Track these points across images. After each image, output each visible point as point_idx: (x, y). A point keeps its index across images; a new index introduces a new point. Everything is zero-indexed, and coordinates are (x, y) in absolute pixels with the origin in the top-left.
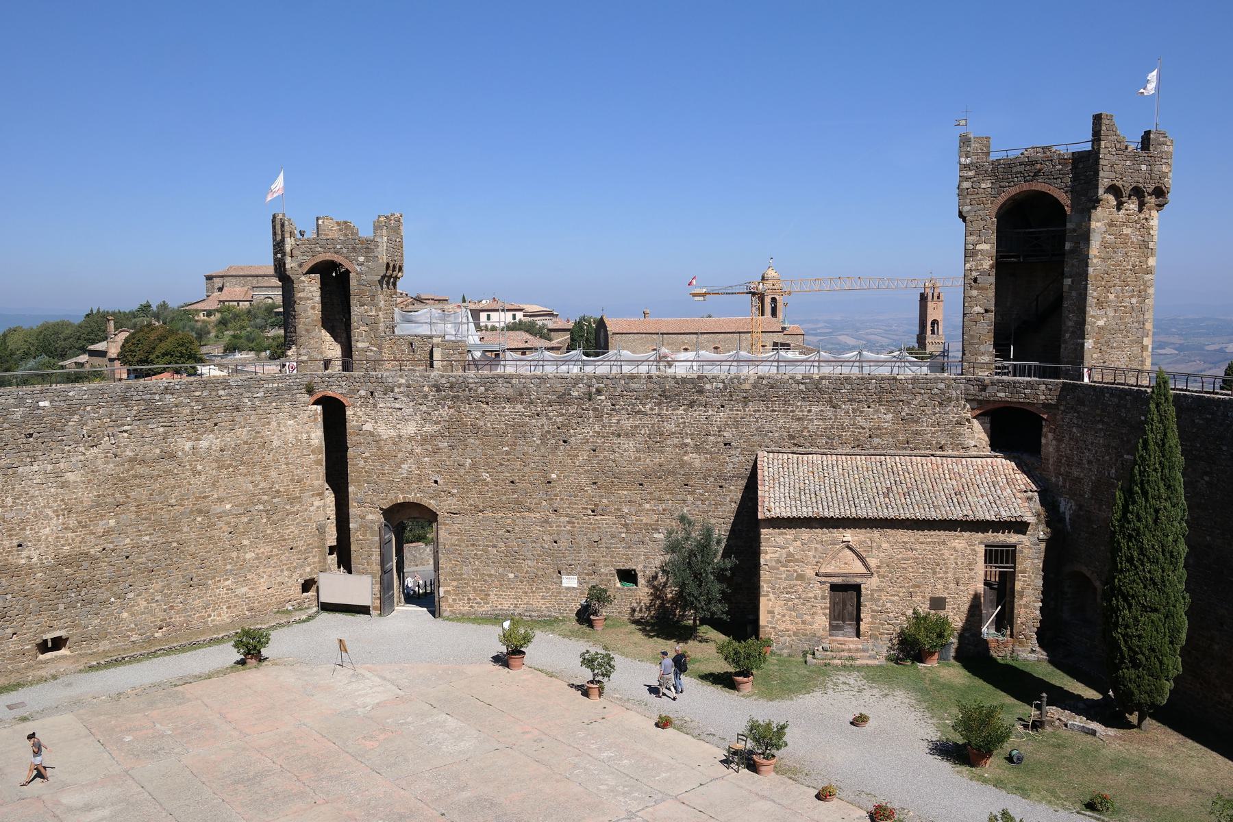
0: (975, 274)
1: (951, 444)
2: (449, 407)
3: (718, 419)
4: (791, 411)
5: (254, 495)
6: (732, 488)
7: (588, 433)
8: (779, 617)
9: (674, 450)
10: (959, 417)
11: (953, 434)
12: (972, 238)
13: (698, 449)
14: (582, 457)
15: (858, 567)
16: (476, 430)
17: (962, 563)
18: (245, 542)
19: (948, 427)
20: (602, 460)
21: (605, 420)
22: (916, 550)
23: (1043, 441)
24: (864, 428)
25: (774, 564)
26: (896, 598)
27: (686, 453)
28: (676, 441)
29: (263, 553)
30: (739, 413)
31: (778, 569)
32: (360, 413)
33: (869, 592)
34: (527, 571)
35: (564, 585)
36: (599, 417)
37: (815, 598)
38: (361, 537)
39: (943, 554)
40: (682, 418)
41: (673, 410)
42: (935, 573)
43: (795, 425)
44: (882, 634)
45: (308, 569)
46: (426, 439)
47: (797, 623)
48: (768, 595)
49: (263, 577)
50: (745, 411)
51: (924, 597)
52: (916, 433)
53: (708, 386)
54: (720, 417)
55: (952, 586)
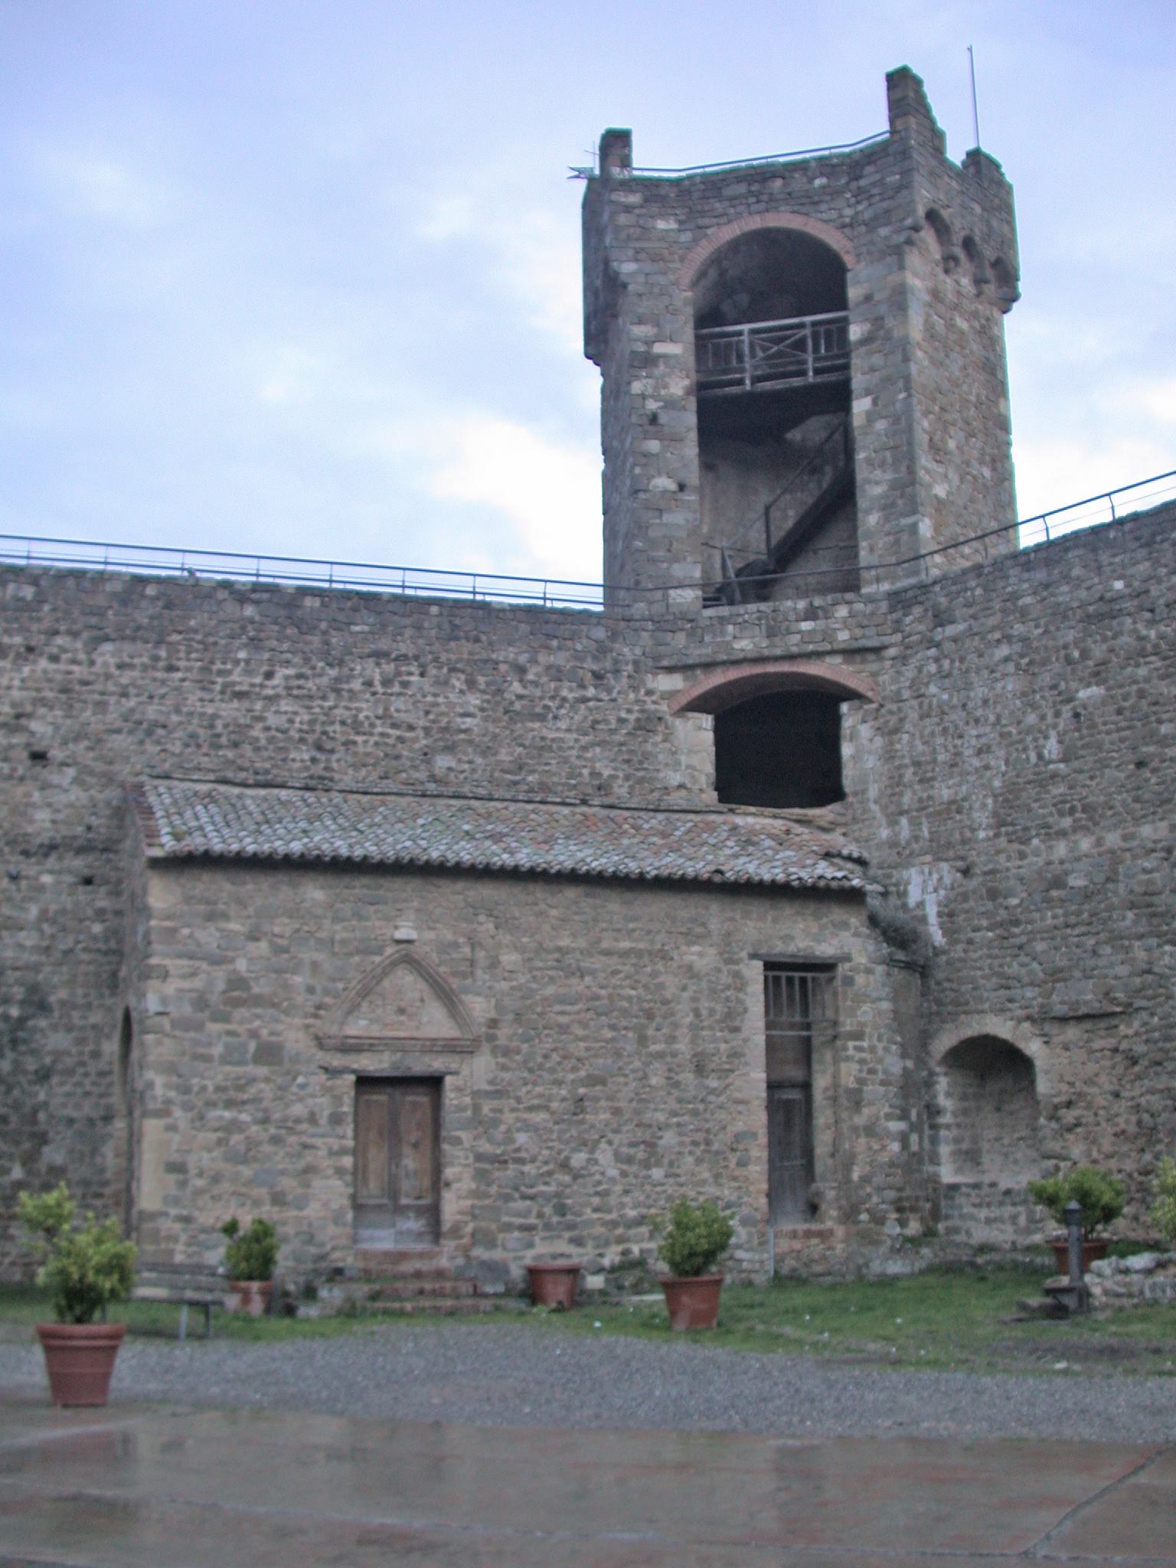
0: (652, 405)
1: (627, 778)
8: (200, 1183)
10: (642, 711)
15: (436, 1022)
17: (712, 1012)
19: (619, 738)
22: (592, 973)
23: (847, 750)
24: (411, 728)
25: (187, 1009)
26: (539, 1117)
31: (200, 1027)
33: (468, 1100)
37: (312, 1119)
39: (661, 986)
42: (643, 1040)
43: (230, 710)
44: (508, 1227)
47: (257, 1203)
48: (164, 1113)
50: (92, 663)
52: (543, 747)
55: (688, 1077)
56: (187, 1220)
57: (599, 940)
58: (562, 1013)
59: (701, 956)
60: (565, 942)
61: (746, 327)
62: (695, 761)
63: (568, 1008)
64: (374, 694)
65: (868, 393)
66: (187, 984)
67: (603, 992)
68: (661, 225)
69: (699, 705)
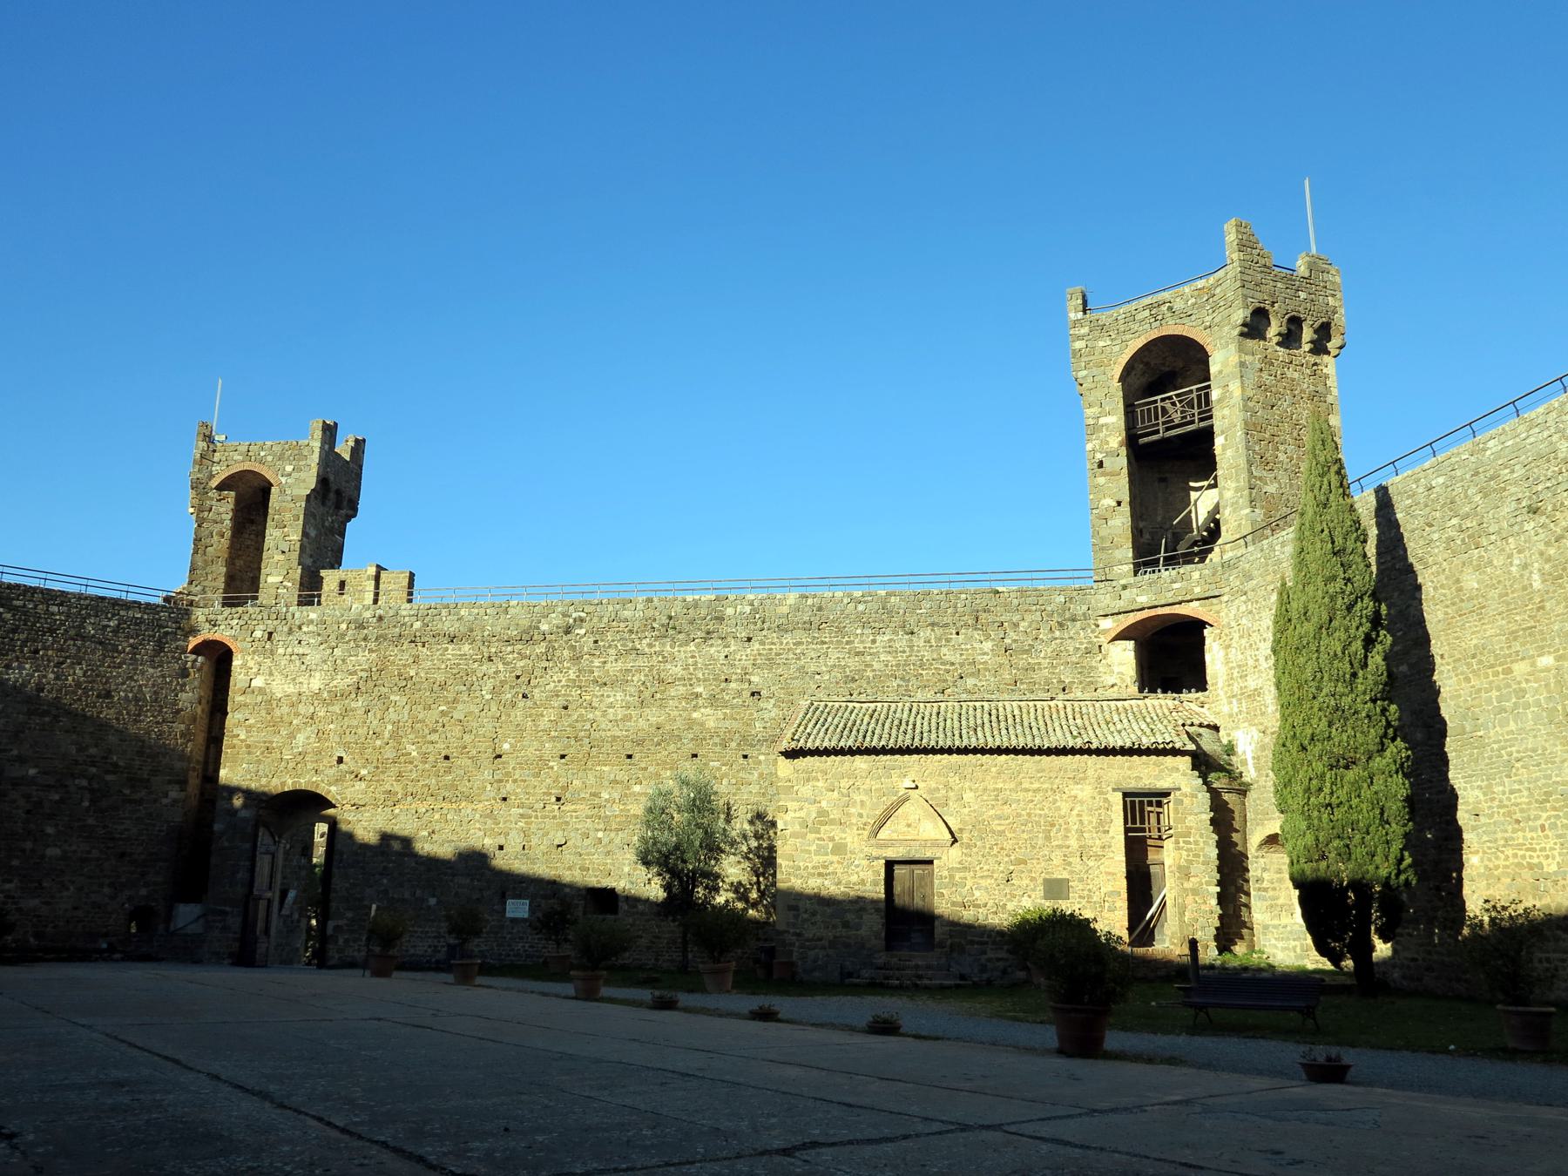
0: (1099, 456)
2: (371, 651)
3: (744, 657)
4: (847, 643)
5: (76, 762)
6: (762, 758)
7: (560, 681)
8: (805, 916)
9: (680, 703)
10: (1088, 643)
11: (1082, 667)
12: (1092, 410)
13: (713, 701)
14: (550, 715)
16: (405, 684)
18: (50, 830)
19: (1074, 659)
20: (577, 721)
21: (584, 662)
24: (953, 664)
25: (797, 827)
27: (696, 708)
28: (682, 690)
29: (75, 851)
30: (773, 647)
31: (804, 836)
32: (251, 664)
34: (457, 894)
35: (508, 915)
36: (576, 659)
38: (226, 844)
39: (1059, 809)
40: (693, 657)
41: (680, 646)
42: (1048, 838)
43: (853, 663)
44: (972, 943)
45: (143, 892)
46: (336, 696)
47: (834, 927)
49: (68, 889)
50: (781, 643)
51: (1033, 879)
52: (1030, 668)
53: (730, 611)
54: (744, 655)
55: (1075, 860)
56: (799, 935)
57: (1021, 783)
58: (1000, 825)
59: (1085, 792)
60: (1000, 785)
61: (1158, 397)
62: (1122, 669)
63: (1003, 822)
64: (931, 646)
65: (1223, 432)
66: (797, 815)
67: (1023, 812)
68: (1101, 344)
69: (1122, 636)
